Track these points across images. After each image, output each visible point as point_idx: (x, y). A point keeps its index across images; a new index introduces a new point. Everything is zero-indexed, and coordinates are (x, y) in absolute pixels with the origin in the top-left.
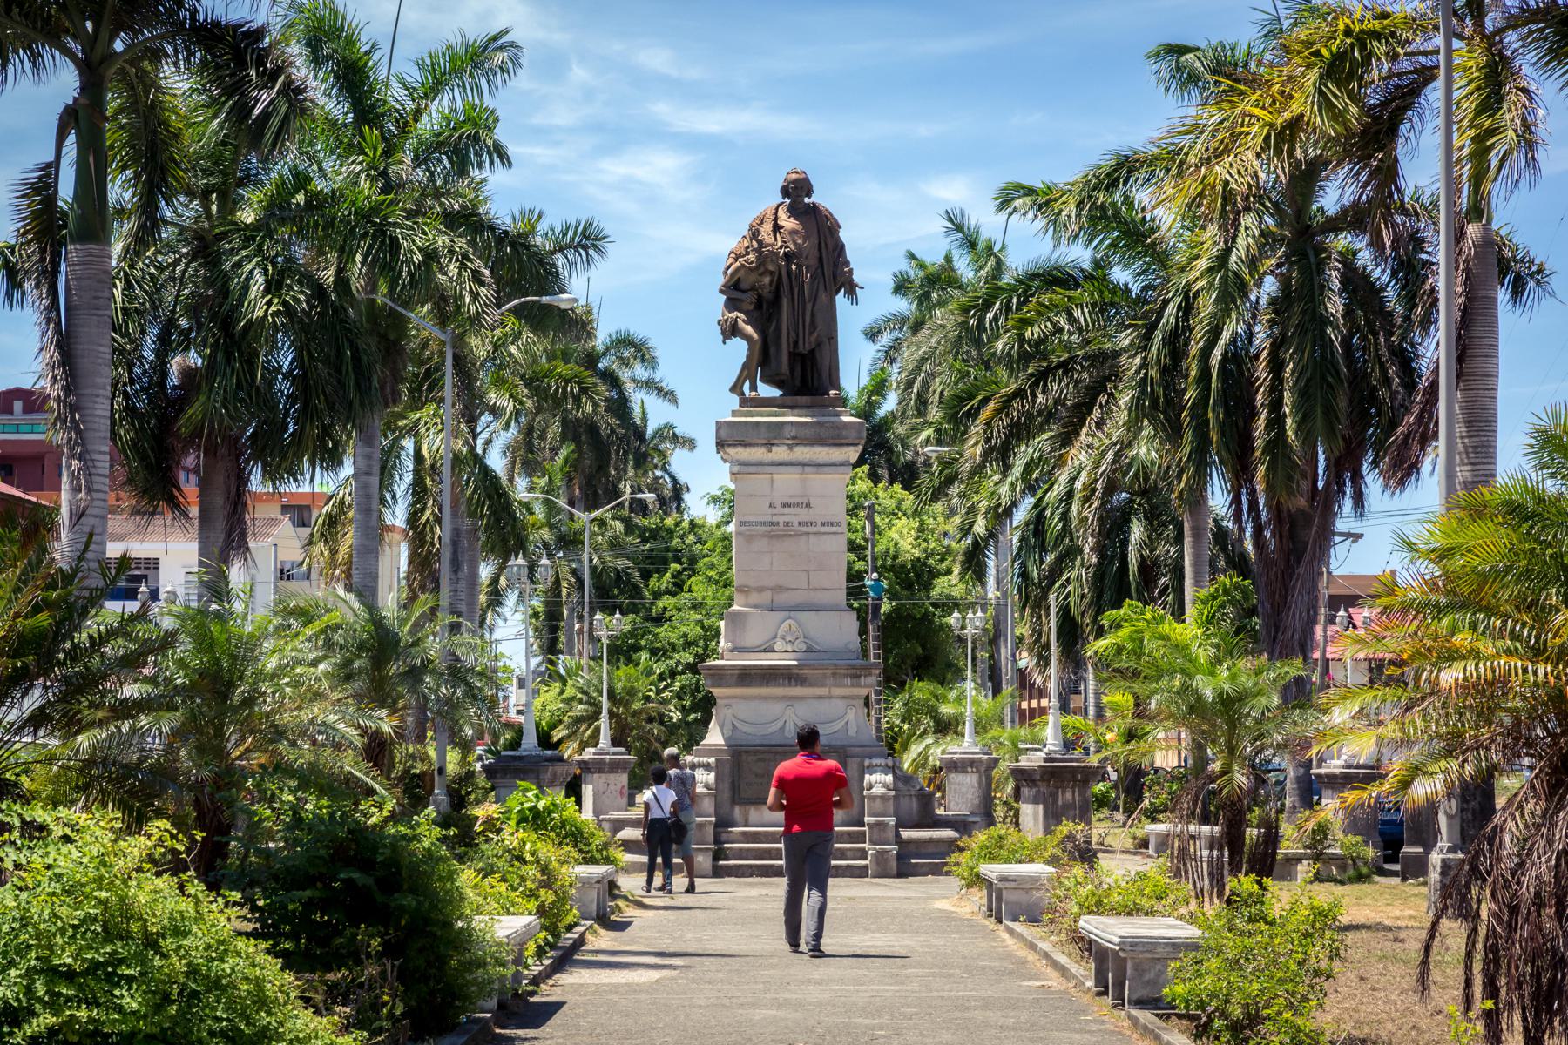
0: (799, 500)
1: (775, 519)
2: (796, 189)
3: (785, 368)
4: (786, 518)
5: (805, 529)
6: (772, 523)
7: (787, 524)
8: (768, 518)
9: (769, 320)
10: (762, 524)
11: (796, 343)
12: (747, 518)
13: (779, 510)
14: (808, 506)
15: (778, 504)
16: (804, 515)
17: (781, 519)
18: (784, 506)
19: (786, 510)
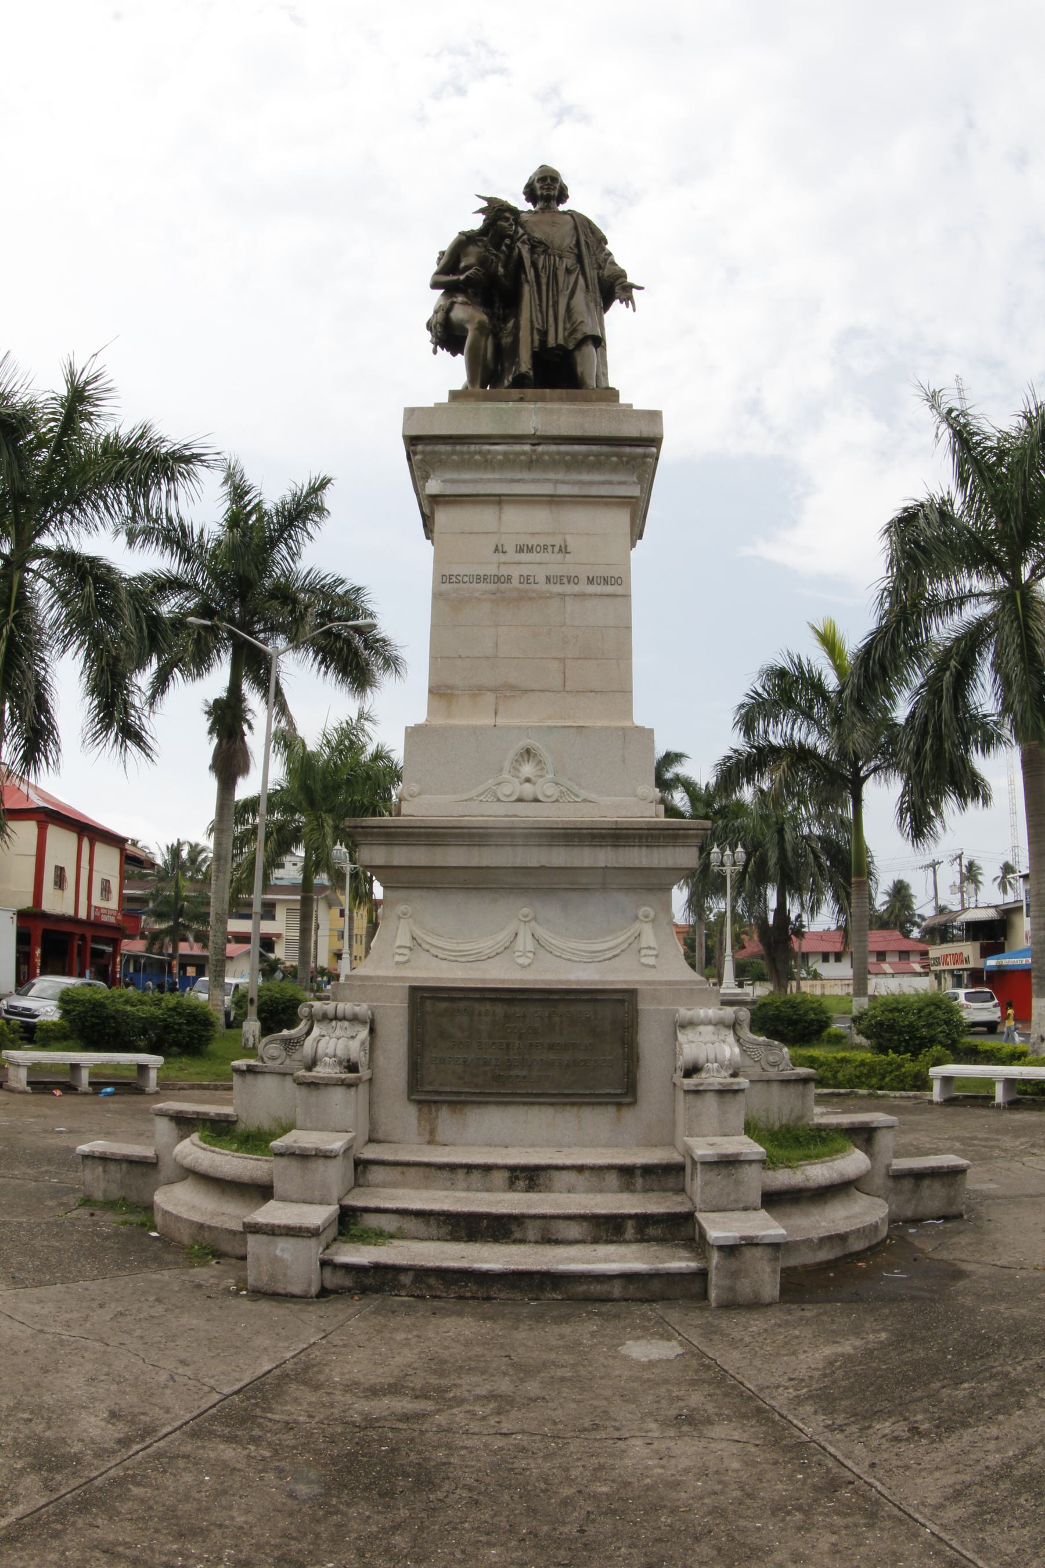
0: (542, 541)
1: (504, 571)
2: (547, 188)
3: (525, 364)
4: (525, 571)
5: (557, 588)
6: (498, 579)
7: (526, 579)
8: (491, 570)
9: (505, 320)
10: (480, 579)
11: (543, 341)
12: (456, 570)
13: (512, 555)
14: (564, 550)
15: (510, 548)
16: (555, 564)
17: (515, 572)
18: (520, 549)
19: (525, 557)
